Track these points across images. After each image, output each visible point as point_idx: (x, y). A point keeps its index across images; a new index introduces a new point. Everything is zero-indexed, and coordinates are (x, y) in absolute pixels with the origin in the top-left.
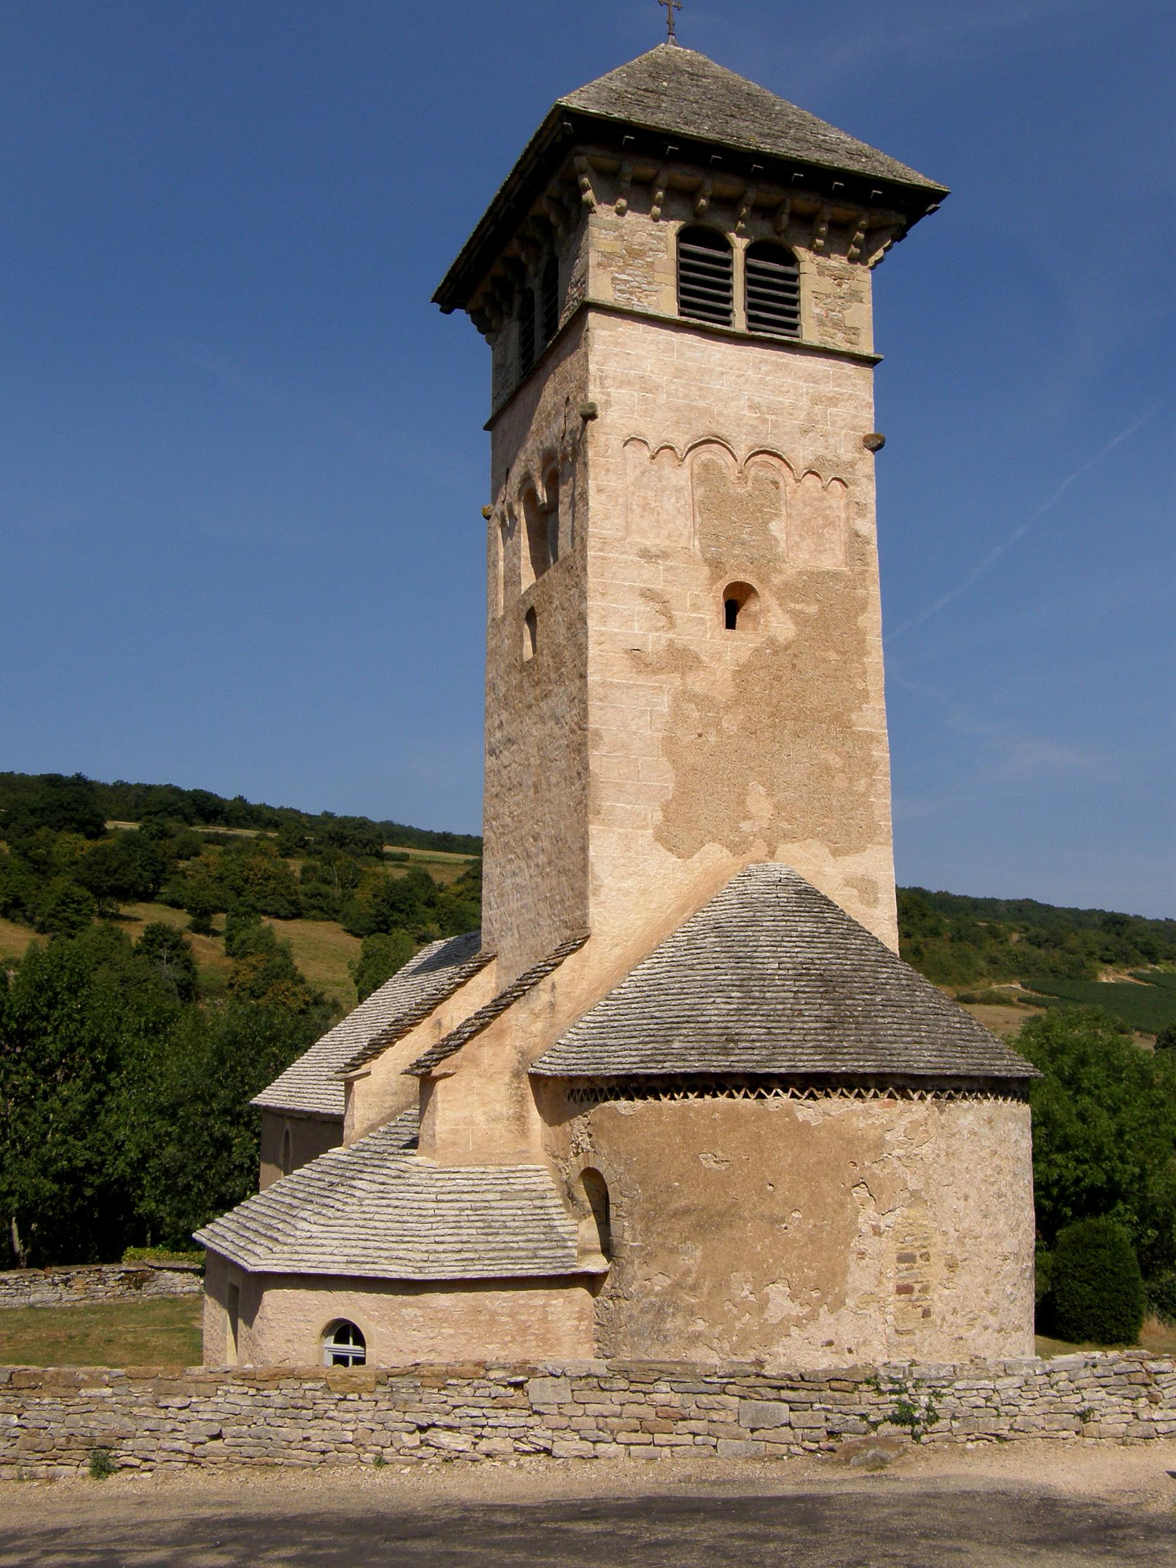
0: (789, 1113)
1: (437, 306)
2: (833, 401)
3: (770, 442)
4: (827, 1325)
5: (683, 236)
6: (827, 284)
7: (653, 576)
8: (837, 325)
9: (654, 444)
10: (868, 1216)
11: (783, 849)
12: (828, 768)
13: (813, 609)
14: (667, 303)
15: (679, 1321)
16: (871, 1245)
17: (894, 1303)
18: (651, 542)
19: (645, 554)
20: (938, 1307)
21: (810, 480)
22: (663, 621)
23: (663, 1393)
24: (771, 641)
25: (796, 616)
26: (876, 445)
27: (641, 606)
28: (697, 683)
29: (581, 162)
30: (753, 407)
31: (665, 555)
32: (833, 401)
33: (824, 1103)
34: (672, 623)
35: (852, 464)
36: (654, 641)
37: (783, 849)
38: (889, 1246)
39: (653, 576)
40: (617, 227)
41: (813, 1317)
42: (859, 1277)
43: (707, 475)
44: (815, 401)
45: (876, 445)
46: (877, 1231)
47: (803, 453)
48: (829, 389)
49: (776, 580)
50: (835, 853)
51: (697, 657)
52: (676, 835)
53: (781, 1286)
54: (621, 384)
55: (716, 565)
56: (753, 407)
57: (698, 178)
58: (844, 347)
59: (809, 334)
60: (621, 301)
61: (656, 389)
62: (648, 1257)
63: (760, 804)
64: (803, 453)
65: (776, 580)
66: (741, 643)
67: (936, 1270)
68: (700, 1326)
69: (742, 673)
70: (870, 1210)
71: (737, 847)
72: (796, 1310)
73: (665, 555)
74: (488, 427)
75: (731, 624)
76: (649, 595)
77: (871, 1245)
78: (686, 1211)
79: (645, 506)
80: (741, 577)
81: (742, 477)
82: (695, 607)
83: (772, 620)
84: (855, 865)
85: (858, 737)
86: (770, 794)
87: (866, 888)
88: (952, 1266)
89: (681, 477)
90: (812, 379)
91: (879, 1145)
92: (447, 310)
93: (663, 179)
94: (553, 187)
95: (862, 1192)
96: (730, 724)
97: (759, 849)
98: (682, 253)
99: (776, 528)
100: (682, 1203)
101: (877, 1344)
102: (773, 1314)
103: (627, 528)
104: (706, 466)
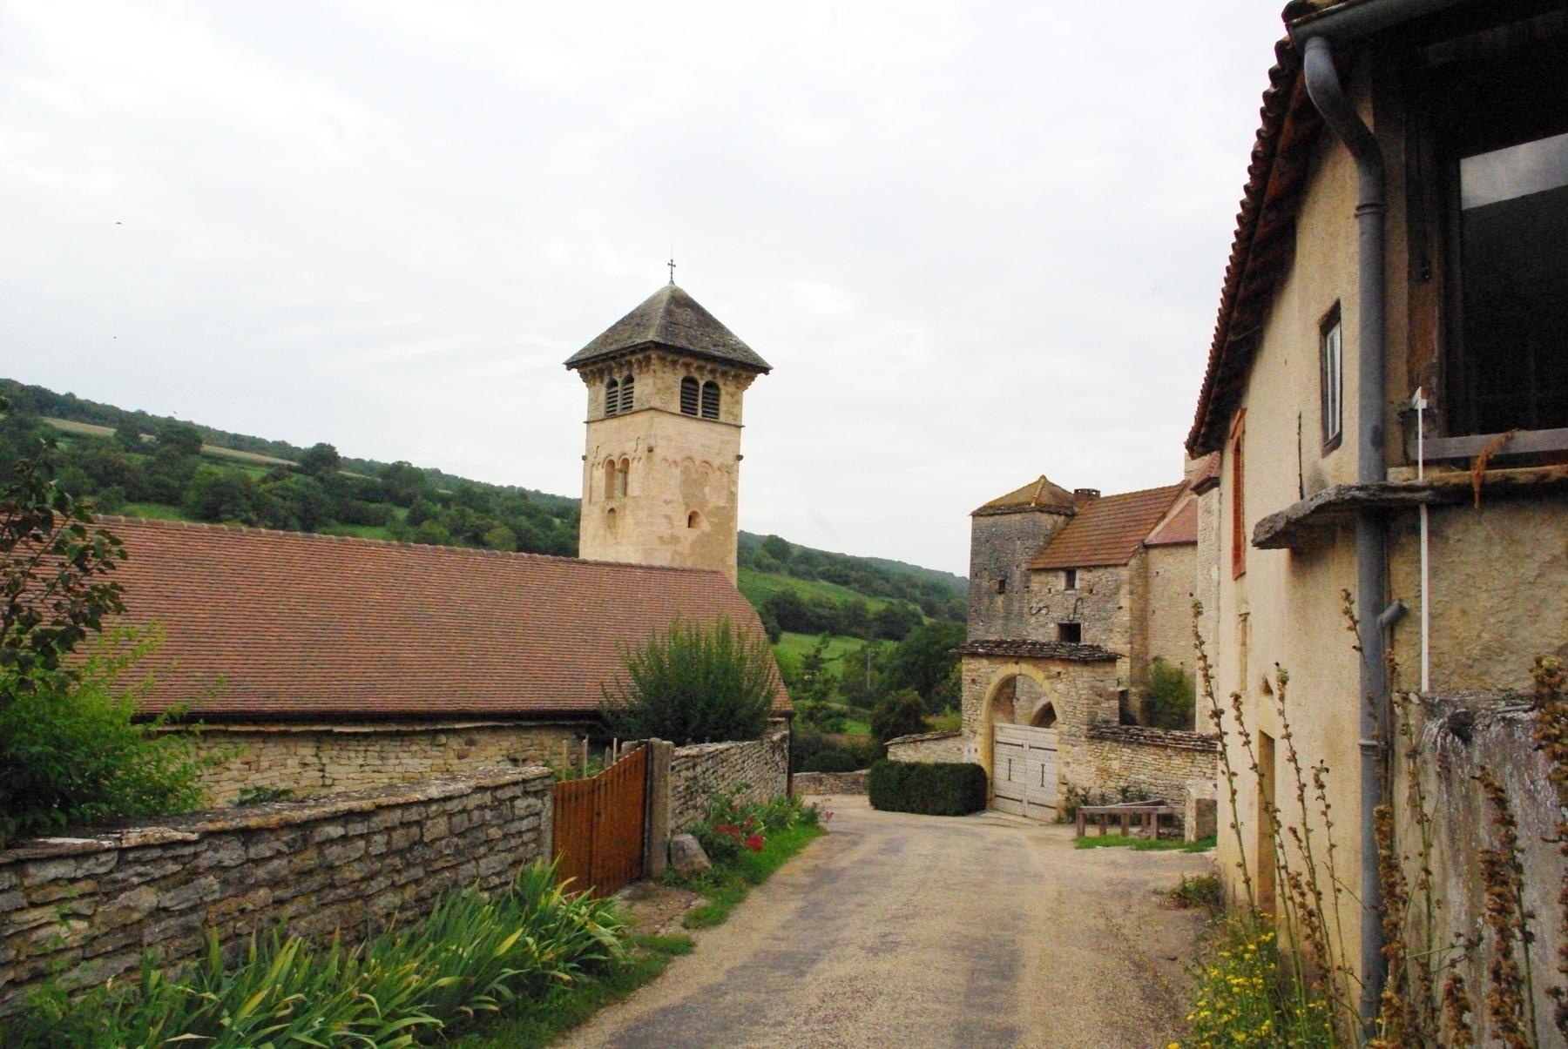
7: (667, 510)
14: (676, 406)
26: (740, 458)
27: (664, 521)
28: (679, 548)
36: (667, 533)
39: (667, 510)
43: (686, 471)
45: (740, 458)
47: (717, 462)
55: (687, 505)
59: (722, 417)
64: (717, 462)
69: (694, 543)
76: (666, 517)
83: (704, 525)
89: (677, 472)
94: (640, 356)
99: (706, 490)
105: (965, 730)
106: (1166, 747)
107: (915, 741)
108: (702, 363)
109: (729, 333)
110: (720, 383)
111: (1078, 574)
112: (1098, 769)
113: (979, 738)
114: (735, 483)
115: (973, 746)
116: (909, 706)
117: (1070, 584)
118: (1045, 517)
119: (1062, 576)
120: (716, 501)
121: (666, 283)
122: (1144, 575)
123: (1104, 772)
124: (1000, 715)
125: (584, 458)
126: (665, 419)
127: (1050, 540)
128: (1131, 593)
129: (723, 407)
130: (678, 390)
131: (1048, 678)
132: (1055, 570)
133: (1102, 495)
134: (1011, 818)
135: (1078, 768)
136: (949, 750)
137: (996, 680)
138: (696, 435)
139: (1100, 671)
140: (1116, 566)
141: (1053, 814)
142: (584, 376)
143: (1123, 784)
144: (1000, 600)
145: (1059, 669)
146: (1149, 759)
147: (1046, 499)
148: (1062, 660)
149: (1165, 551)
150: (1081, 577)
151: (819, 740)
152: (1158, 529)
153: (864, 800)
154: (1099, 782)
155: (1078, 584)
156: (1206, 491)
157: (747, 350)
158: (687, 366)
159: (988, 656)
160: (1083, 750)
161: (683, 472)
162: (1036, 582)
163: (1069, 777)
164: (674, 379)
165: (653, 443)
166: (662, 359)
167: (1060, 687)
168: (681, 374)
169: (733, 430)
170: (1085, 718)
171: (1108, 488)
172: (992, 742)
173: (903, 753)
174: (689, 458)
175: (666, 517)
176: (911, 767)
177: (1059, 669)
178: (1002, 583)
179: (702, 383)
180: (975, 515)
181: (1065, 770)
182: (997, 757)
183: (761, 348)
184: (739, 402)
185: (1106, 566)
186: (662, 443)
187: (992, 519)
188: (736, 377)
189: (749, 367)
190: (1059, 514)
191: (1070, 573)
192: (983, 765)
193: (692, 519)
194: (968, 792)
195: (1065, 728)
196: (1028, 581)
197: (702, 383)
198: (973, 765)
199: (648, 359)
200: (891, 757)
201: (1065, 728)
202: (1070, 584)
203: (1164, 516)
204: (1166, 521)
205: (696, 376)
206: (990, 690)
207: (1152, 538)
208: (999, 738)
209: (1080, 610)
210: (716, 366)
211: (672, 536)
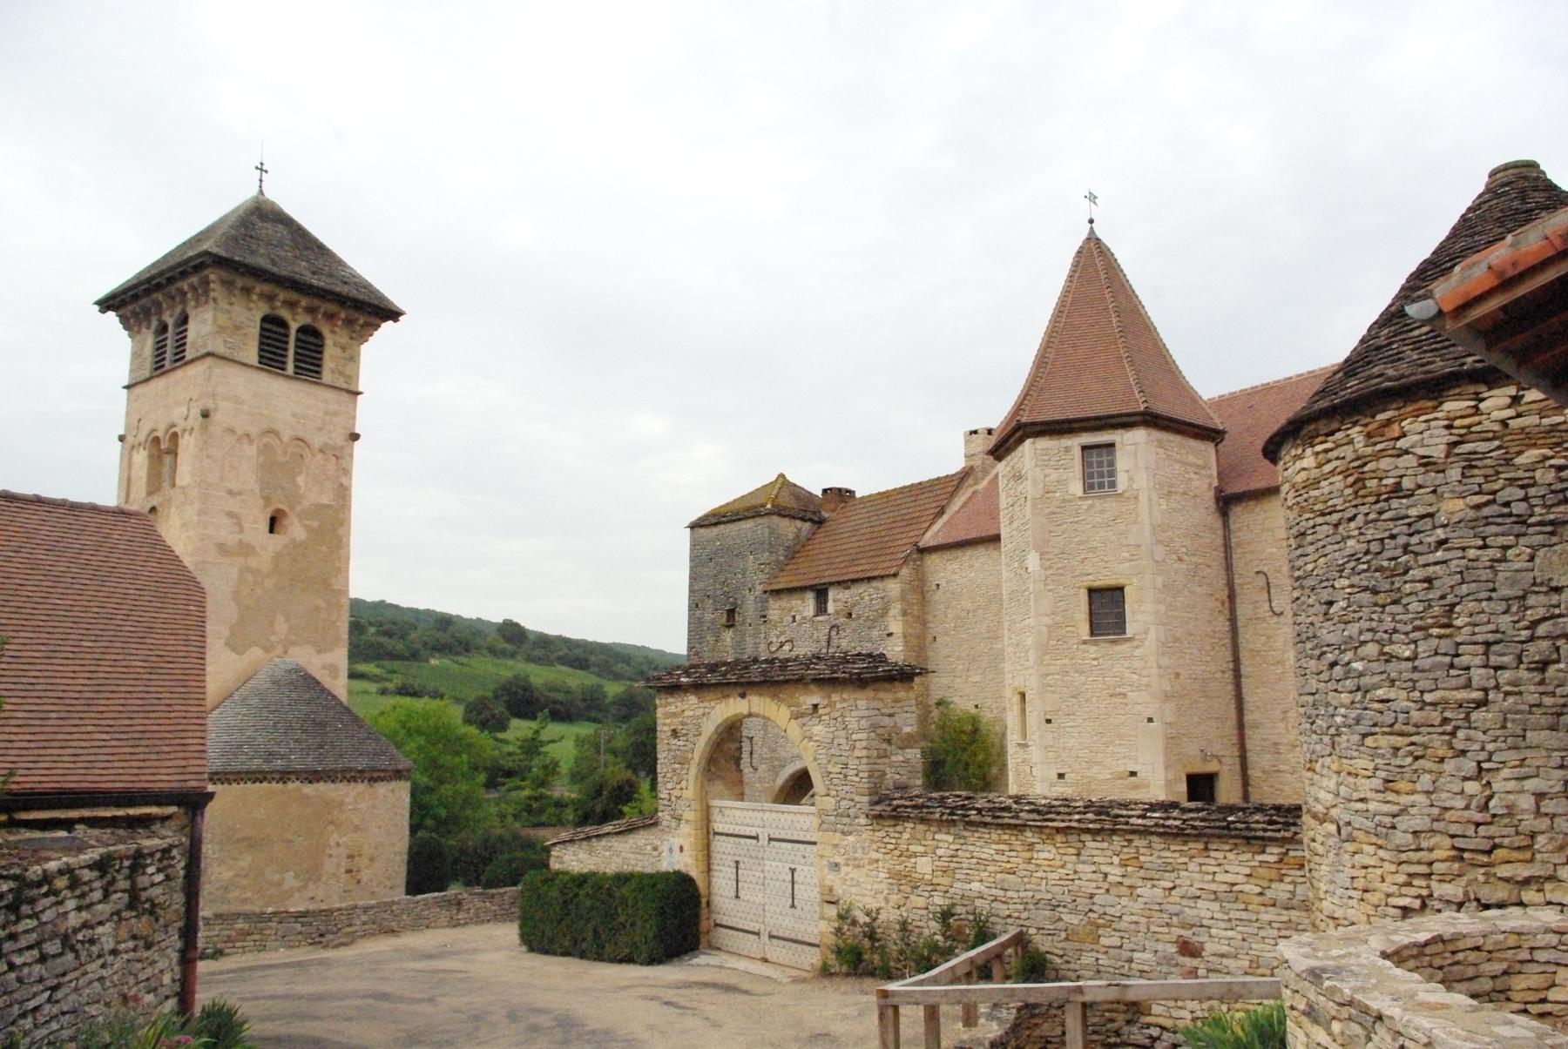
0: (298, 790)
1: (97, 308)
2: (336, 414)
3: (301, 434)
4: (312, 889)
5: (264, 320)
6: (338, 351)
8: (341, 373)
9: (239, 432)
10: (335, 837)
11: (291, 651)
12: (317, 609)
13: (315, 524)
14: (251, 354)
15: (237, 893)
16: (335, 851)
17: (344, 877)
18: (234, 486)
19: (231, 493)
20: (365, 879)
21: (320, 456)
22: (237, 529)
23: (240, 925)
24: (293, 540)
25: (308, 528)
27: (227, 521)
28: (253, 562)
29: (212, 277)
30: (294, 415)
31: (240, 493)
32: (336, 414)
33: (316, 785)
34: (242, 531)
35: (342, 448)
36: (231, 539)
37: (293, 650)
38: (343, 852)
40: (229, 312)
41: (305, 887)
42: (328, 866)
43: (266, 450)
44: (326, 413)
46: (338, 845)
47: (317, 441)
48: (333, 407)
49: (298, 509)
50: (319, 652)
51: (253, 548)
52: (234, 646)
53: (291, 873)
54: (225, 399)
55: (267, 500)
56: (294, 415)
57: (277, 291)
58: (345, 386)
59: (327, 376)
60: (228, 353)
61: (242, 403)
62: (222, 862)
63: (281, 626)
64: (317, 441)
65: (298, 509)
66: (277, 541)
67: (365, 862)
68: (249, 894)
69: (278, 557)
70: (336, 835)
71: (267, 650)
72: (297, 884)
73: (240, 493)
74: (127, 387)
75: (271, 531)
76: (231, 515)
77: (335, 851)
78: (244, 839)
79: (232, 467)
80: (281, 506)
81: (285, 453)
82: (255, 522)
83: (295, 530)
84: (329, 658)
85: (334, 591)
86: (287, 620)
87: (333, 670)
88: (372, 859)
89: (251, 451)
90: (326, 401)
91: (341, 804)
92: (103, 311)
93: (258, 290)
94: (194, 280)
95: (331, 828)
96: (269, 583)
97: (279, 650)
98: (262, 328)
99: (300, 480)
100: (242, 835)
101: (335, 897)
102: (286, 886)
103: (222, 478)
104: (266, 446)
105: (664, 816)
106: (1020, 828)
107: (588, 838)
108: (293, 296)
109: (340, 262)
110: (325, 330)
111: (832, 594)
112: (893, 875)
113: (686, 829)
114: (347, 472)
115: (676, 842)
116: (620, 788)
117: (821, 608)
118: (785, 522)
119: (810, 599)
120: (311, 491)
121: (254, 192)
122: (920, 591)
123: (904, 880)
124: (719, 787)
125: (122, 439)
126: (233, 372)
127: (793, 553)
128: (904, 613)
129: (328, 364)
130: (255, 331)
131: (796, 716)
132: (803, 589)
133: (858, 495)
134: (742, 965)
135: (855, 874)
136: (639, 851)
137: (709, 728)
138: (284, 399)
139: (888, 697)
140: (882, 577)
141: (812, 958)
142: (125, 321)
143: (939, 900)
144: (728, 636)
145: (815, 699)
146: (988, 852)
147: (786, 500)
148: (820, 682)
149: (948, 555)
150: (837, 599)
151: (516, 837)
152: (935, 528)
153: (509, 933)
154: (895, 898)
155: (831, 607)
156: (1009, 451)
157: (367, 286)
158: (270, 298)
159: (698, 687)
160: (864, 840)
161: (260, 452)
162: (776, 609)
163: (839, 891)
164: (250, 316)
165: (210, 405)
166: (227, 284)
167: (818, 730)
168: (261, 310)
169: (345, 396)
170: (865, 785)
171: (863, 488)
172: (708, 834)
173: (575, 858)
174: (275, 433)
175: (231, 515)
176: (582, 880)
177: (815, 699)
178: (731, 613)
179: (294, 327)
180: (694, 526)
181: (831, 878)
182: (717, 858)
183: (390, 289)
184: (354, 359)
185: (870, 579)
186: (223, 404)
187: (715, 530)
188: (349, 322)
189: (376, 311)
190: (803, 519)
191: (821, 593)
192: (694, 874)
193: (274, 524)
194: (671, 921)
195: (829, 803)
196: (765, 608)
197: (294, 327)
198: (677, 873)
199: (206, 282)
200: (555, 865)
201: (829, 803)
202: (821, 608)
203: (942, 512)
204: (945, 517)
205: (285, 313)
206: (701, 746)
207: (928, 539)
208: (718, 827)
209: (835, 642)
210: (316, 302)
211: (240, 543)
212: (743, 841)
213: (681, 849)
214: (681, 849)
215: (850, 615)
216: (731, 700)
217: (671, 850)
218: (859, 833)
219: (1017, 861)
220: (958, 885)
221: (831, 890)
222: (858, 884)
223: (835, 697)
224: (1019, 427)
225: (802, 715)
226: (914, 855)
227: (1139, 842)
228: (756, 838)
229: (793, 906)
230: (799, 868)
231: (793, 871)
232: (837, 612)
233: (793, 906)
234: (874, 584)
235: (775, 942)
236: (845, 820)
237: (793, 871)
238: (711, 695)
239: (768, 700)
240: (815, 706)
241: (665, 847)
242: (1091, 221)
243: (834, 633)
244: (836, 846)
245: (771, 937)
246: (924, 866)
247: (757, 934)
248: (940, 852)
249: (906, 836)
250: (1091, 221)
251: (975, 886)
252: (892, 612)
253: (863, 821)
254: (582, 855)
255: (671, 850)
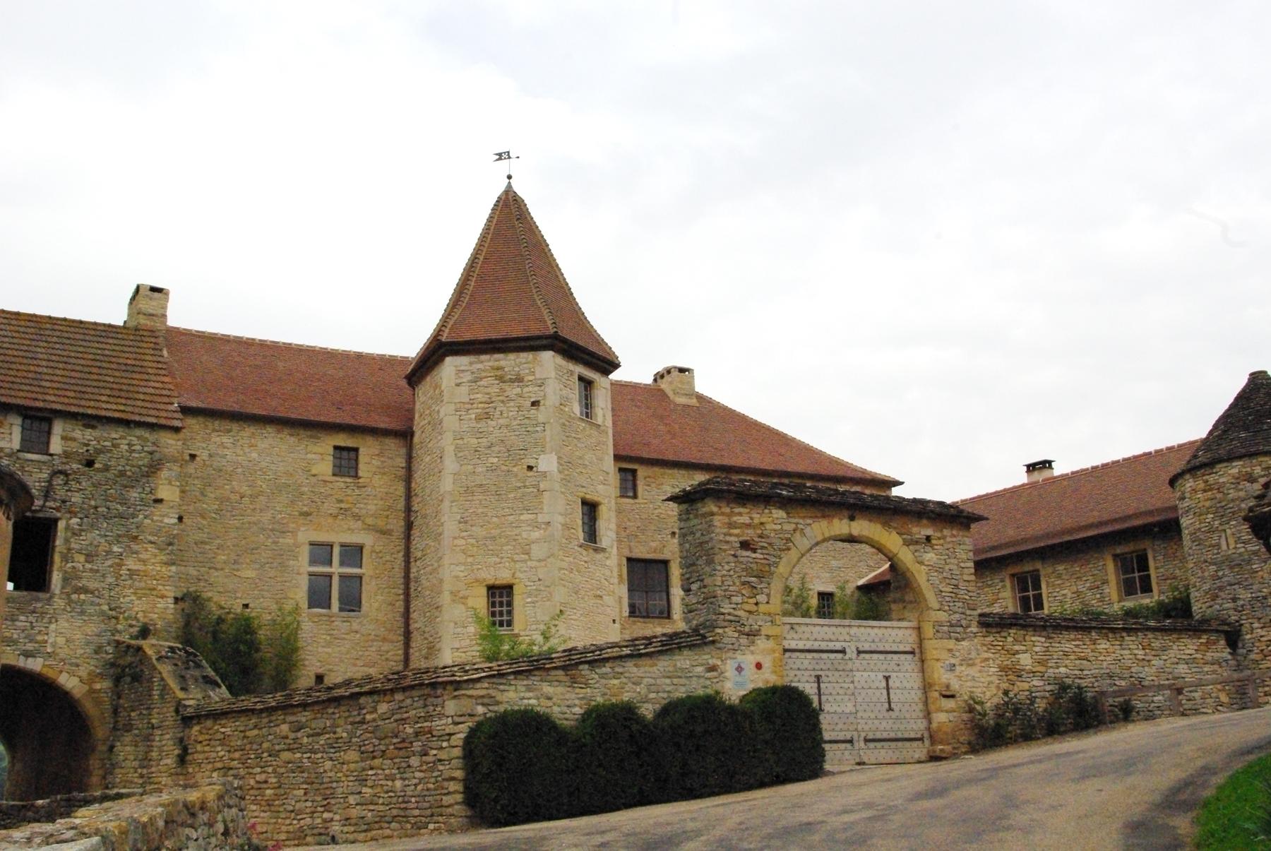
111: (58, 428)
112: (1003, 669)
115: (748, 660)
123: (1012, 671)
131: (907, 543)
135: (973, 671)
136: (686, 674)
145: (929, 532)
146: (1068, 646)
160: (974, 645)
163: (955, 685)
167: (930, 556)
177: (929, 532)
209: (60, 493)
212: (824, 656)
213: (759, 666)
214: (759, 666)
215: (90, 464)
216: (836, 521)
217: (739, 669)
218: (971, 639)
219: (1088, 652)
220: (1051, 670)
221: (948, 686)
222: (973, 679)
223: (946, 532)
224: (556, 337)
225: (917, 543)
226: (1017, 652)
227: (1150, 635)
228: (843, 651)
229: (890, 709)
230: (893, 675)
231: (887, 678)
232: (67, 455)
233: (890, 709)
234: (138, 432)
235: (872, 745)
236: (959, 629)
237: (887, 678)
238: (803, 512)
239: (879, 527)
240: (928, 538)
241: (729, 668)
242: (509, 177)
243: (59, 480)
244: (950, 650)
245: (867, 741)
246: (1025, 660)
247: (851, 741)
248: (1037, 649)
249: (1010, 639)
250: (509, 177)
251: (1063, 670)
252: (164, 474)
253: (974, 629)
254: (547, 689)
255: (739, 669)
